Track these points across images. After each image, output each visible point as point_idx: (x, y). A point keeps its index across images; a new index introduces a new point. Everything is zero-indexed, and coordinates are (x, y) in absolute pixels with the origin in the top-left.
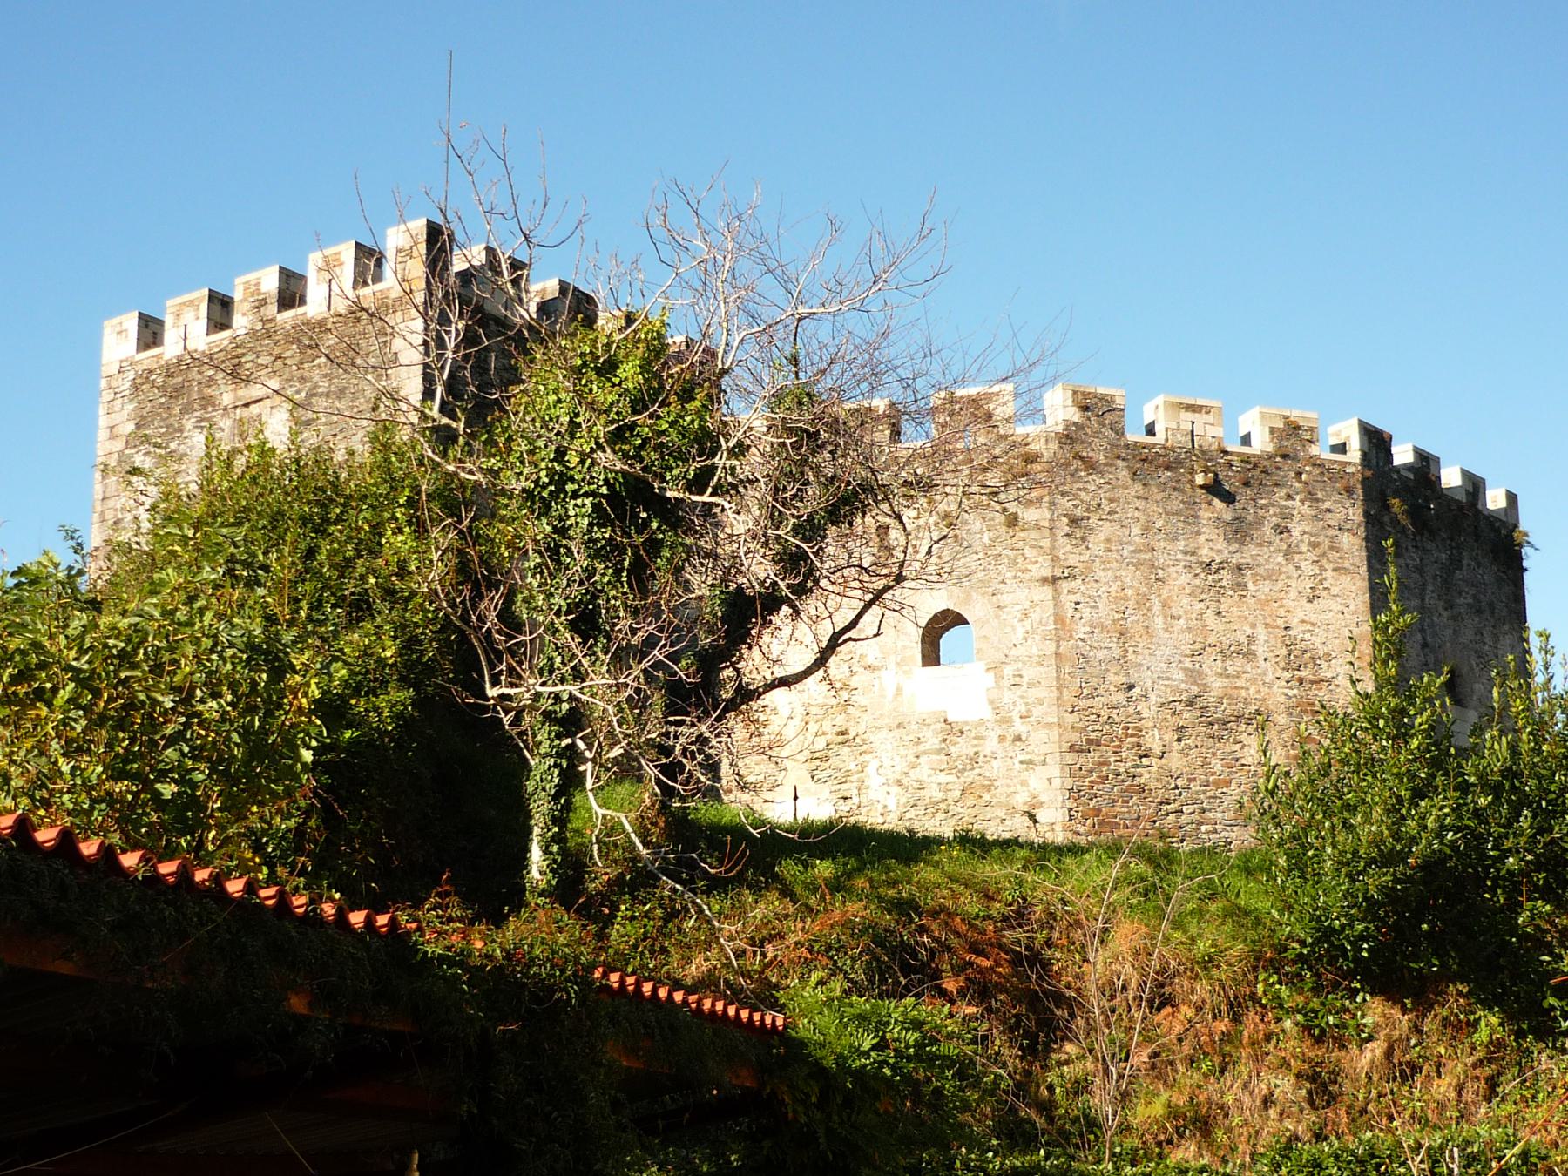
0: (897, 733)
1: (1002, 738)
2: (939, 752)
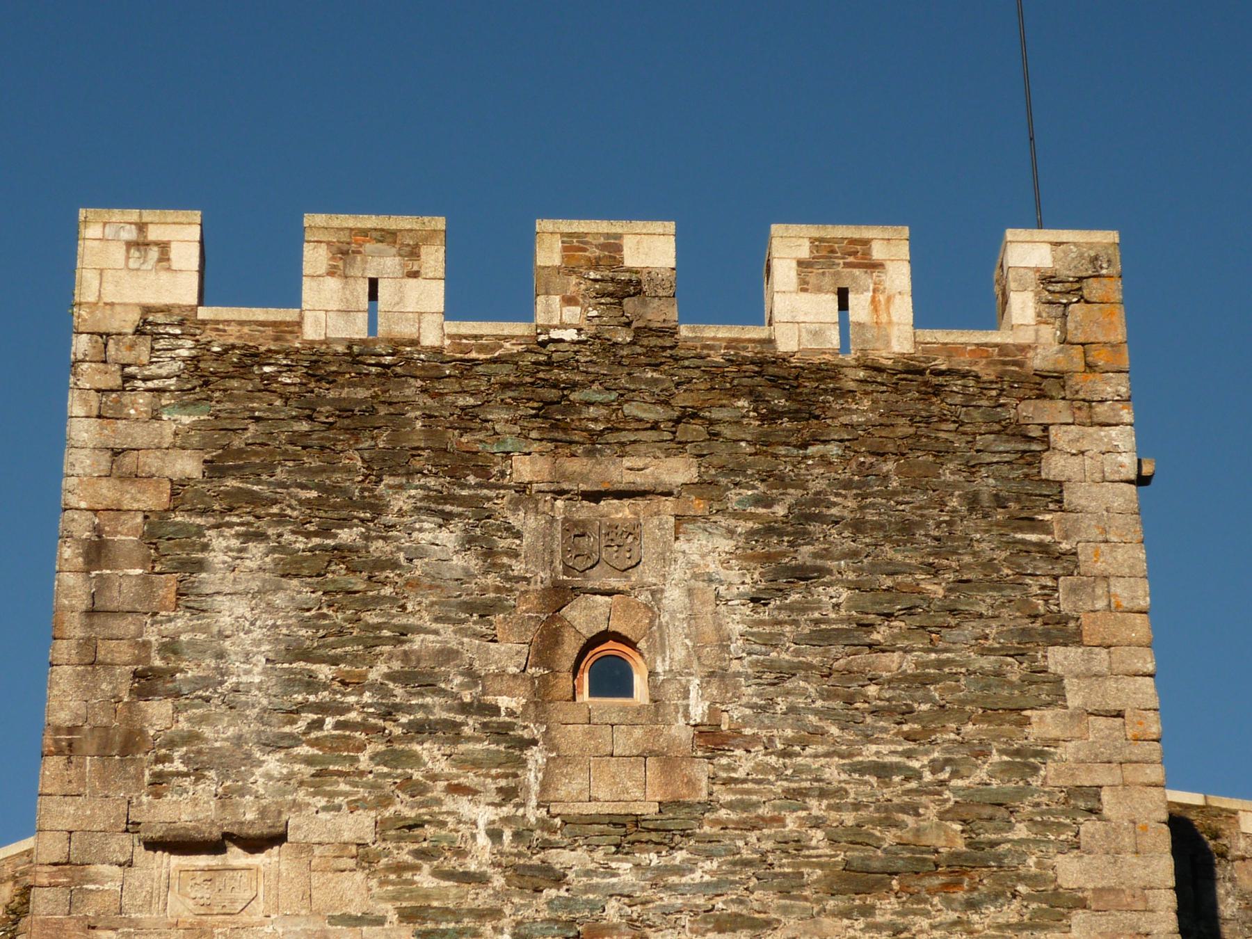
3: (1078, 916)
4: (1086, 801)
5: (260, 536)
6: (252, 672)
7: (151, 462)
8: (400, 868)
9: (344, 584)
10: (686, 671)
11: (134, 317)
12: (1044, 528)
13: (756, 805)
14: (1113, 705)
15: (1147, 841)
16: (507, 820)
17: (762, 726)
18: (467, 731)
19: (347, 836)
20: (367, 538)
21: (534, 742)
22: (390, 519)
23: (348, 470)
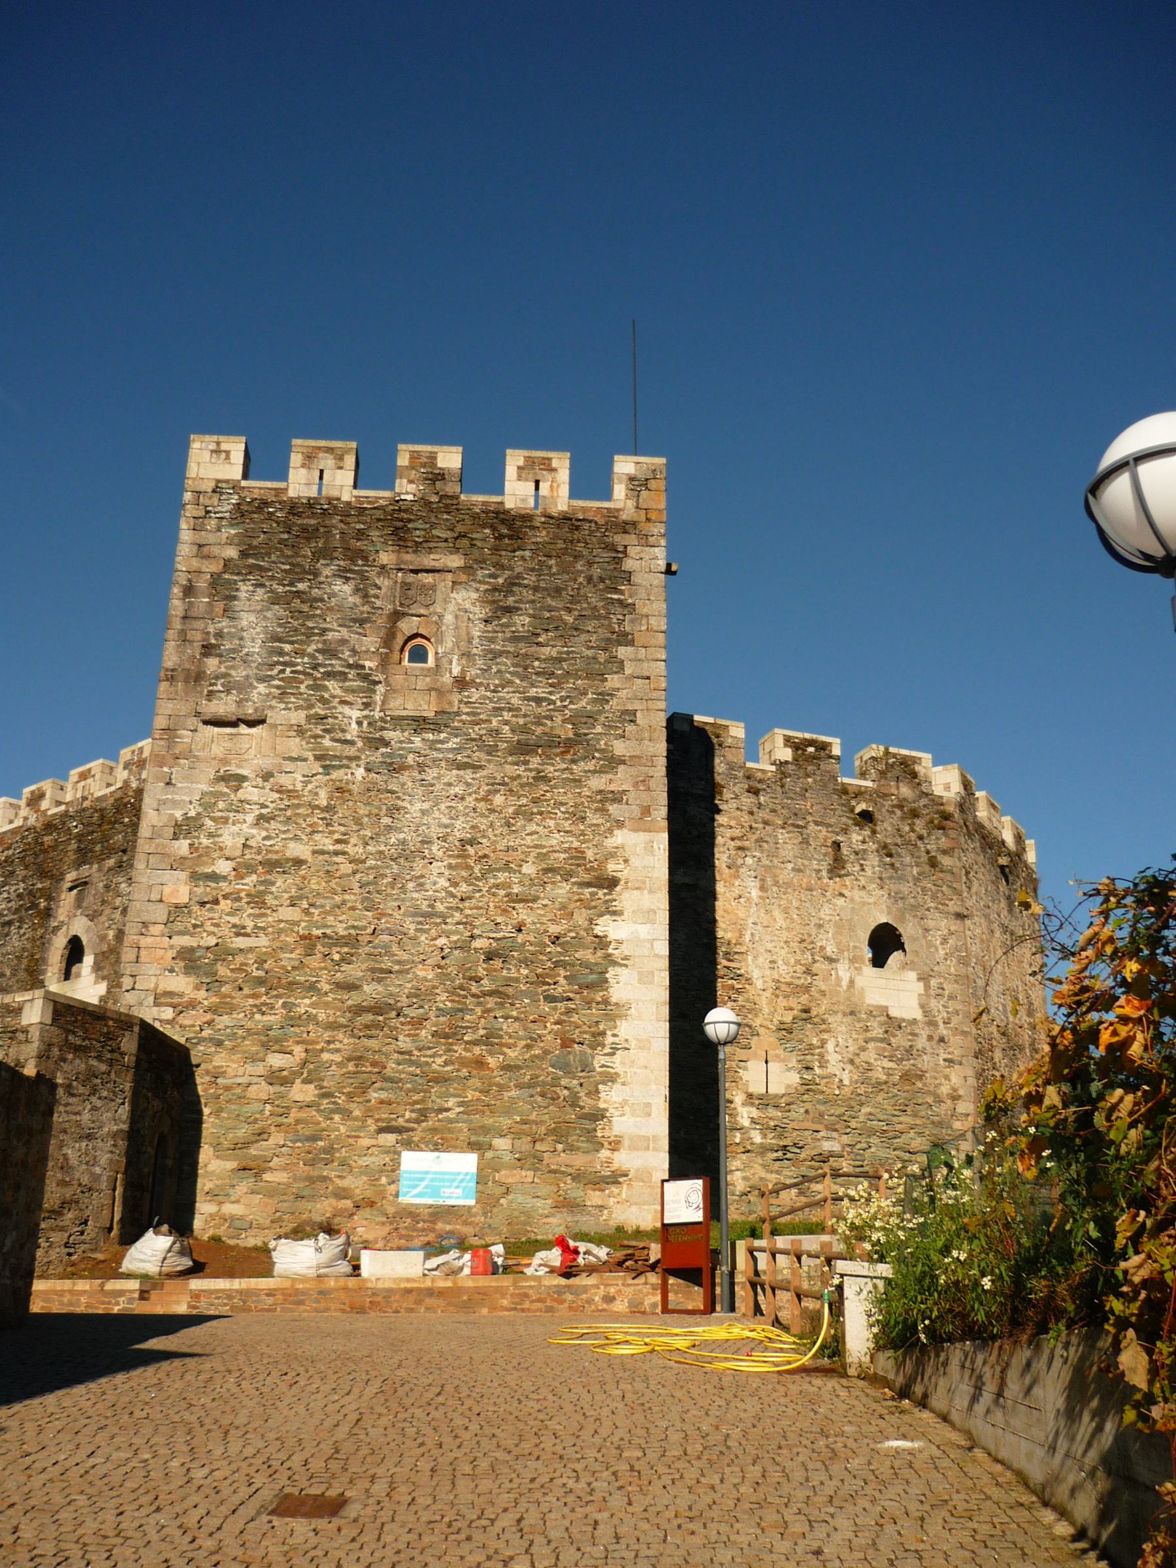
0: (849, 1019)
1: (930, 1038)
2: (882, 1040)
3: (621, 768)
4: (630, 716)
5: (262, 585)
6: (255, 647)
7: (216, 550)
8: (316, 737)
9: (299, 608)
10: (452, 652)
11: (213, 484)
12: (622, 592)
13: (479, 714)
14: (646, 674)
15: (655, 735)
16: (365, 717)
17: (485, 678)
18: (350, 676)
19: (293, 722)
20: (310, 587)
21: (380, 682)
22: (322, 579)
23: (304, 556)
